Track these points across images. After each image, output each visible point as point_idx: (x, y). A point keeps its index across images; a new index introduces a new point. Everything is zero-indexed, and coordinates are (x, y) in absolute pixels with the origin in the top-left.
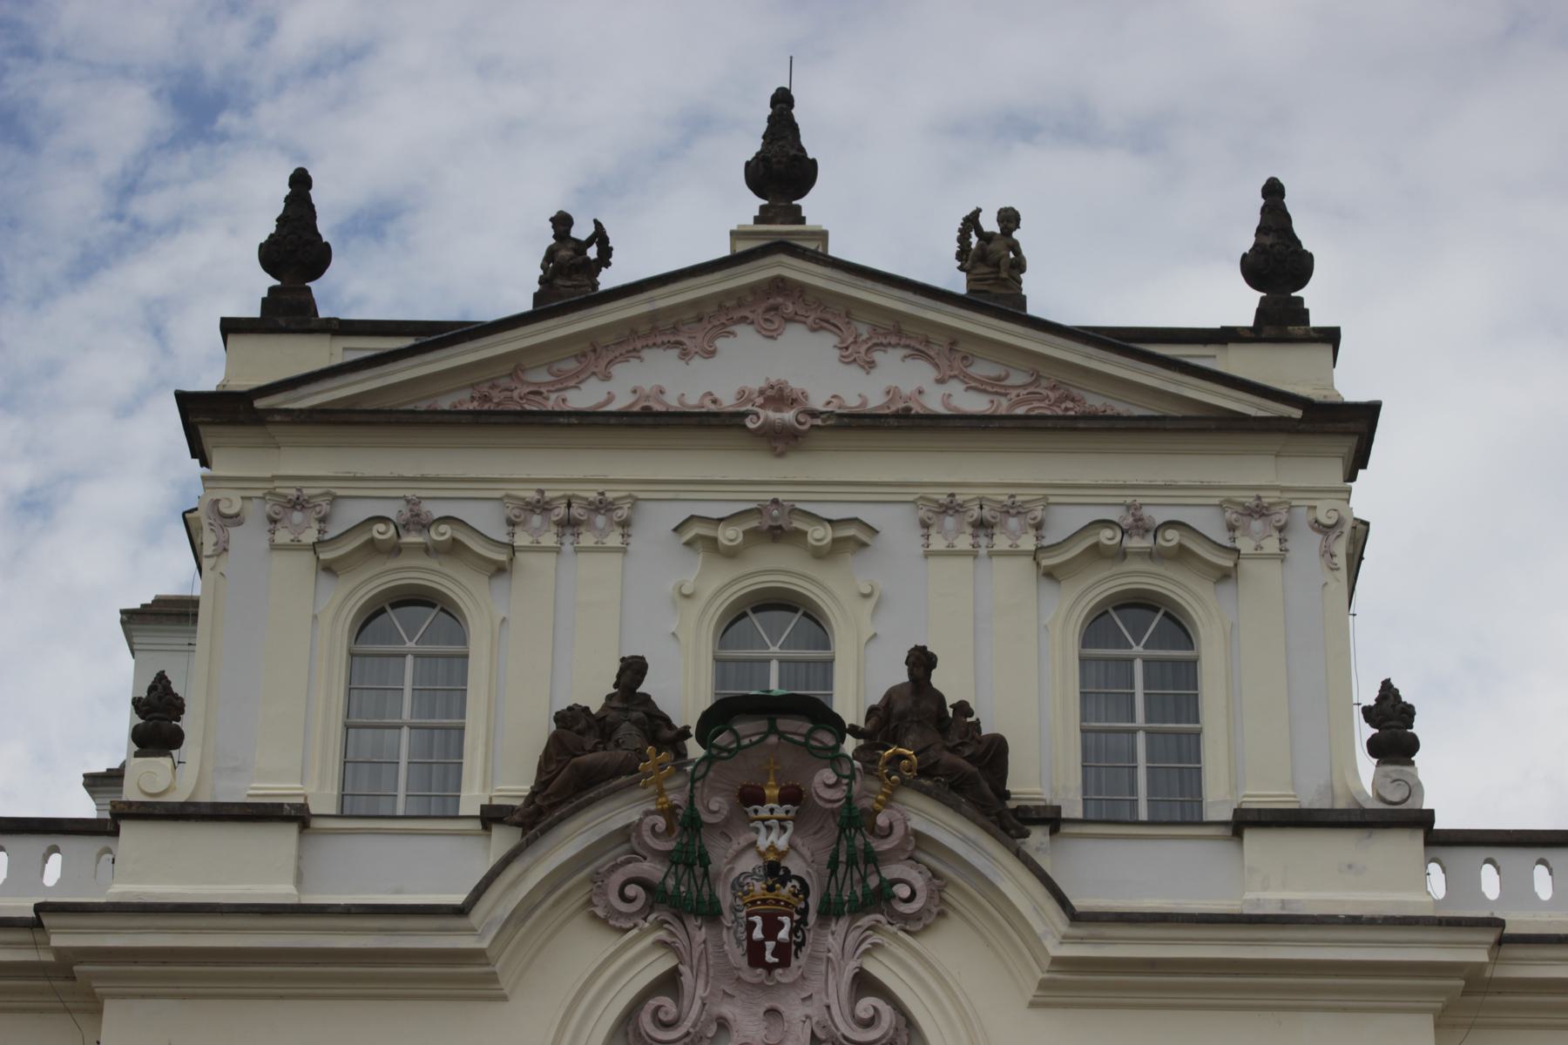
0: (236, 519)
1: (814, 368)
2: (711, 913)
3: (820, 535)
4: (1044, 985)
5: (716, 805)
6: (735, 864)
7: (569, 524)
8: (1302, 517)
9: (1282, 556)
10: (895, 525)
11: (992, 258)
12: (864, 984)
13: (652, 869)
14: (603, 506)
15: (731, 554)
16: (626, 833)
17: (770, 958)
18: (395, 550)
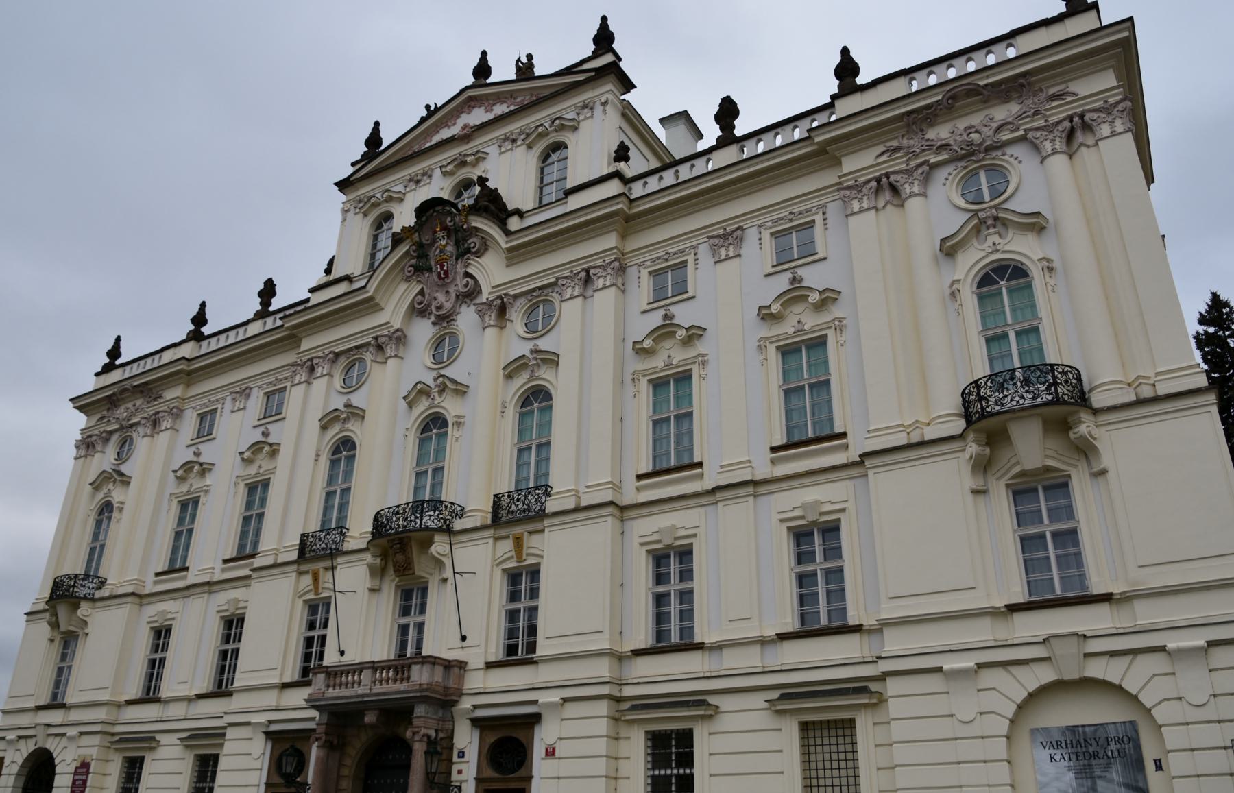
0: (347, 211)
1: (478, 116)
2: (430, 270)
3: (469, 159)
4: (508, 259)
5: (426, 239)
6: (434, 254)
7: (418, 182)
8: (598, 104)
9: (592, 117)
10: (492, 150)
11: (525, 70)
12: (467, 275)
13: (414, 261)
14: (424, 174)
15: (451, 174)
16: (407, 252)
17: (444, 278)
18: (379, 204)
